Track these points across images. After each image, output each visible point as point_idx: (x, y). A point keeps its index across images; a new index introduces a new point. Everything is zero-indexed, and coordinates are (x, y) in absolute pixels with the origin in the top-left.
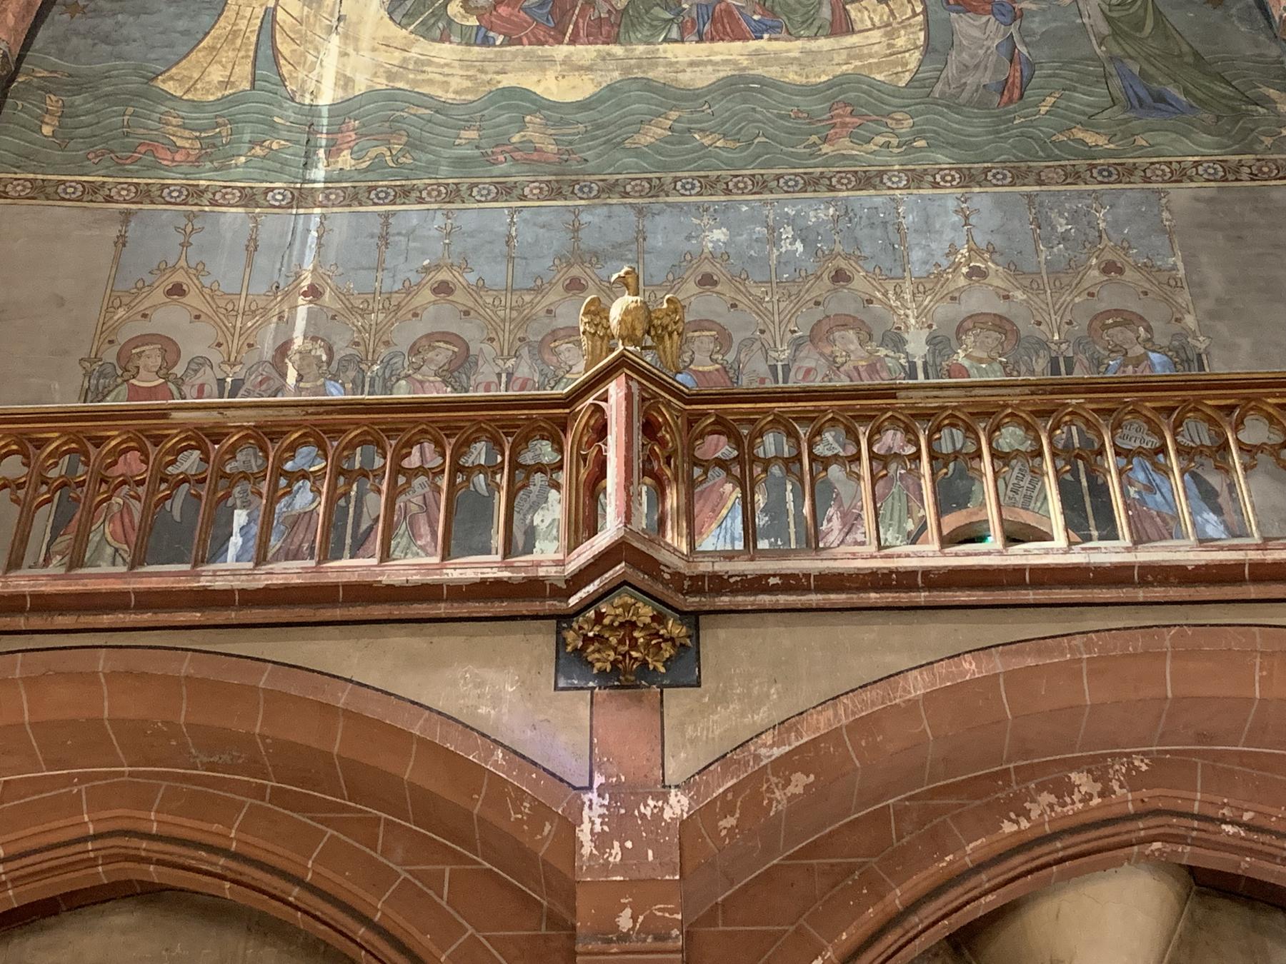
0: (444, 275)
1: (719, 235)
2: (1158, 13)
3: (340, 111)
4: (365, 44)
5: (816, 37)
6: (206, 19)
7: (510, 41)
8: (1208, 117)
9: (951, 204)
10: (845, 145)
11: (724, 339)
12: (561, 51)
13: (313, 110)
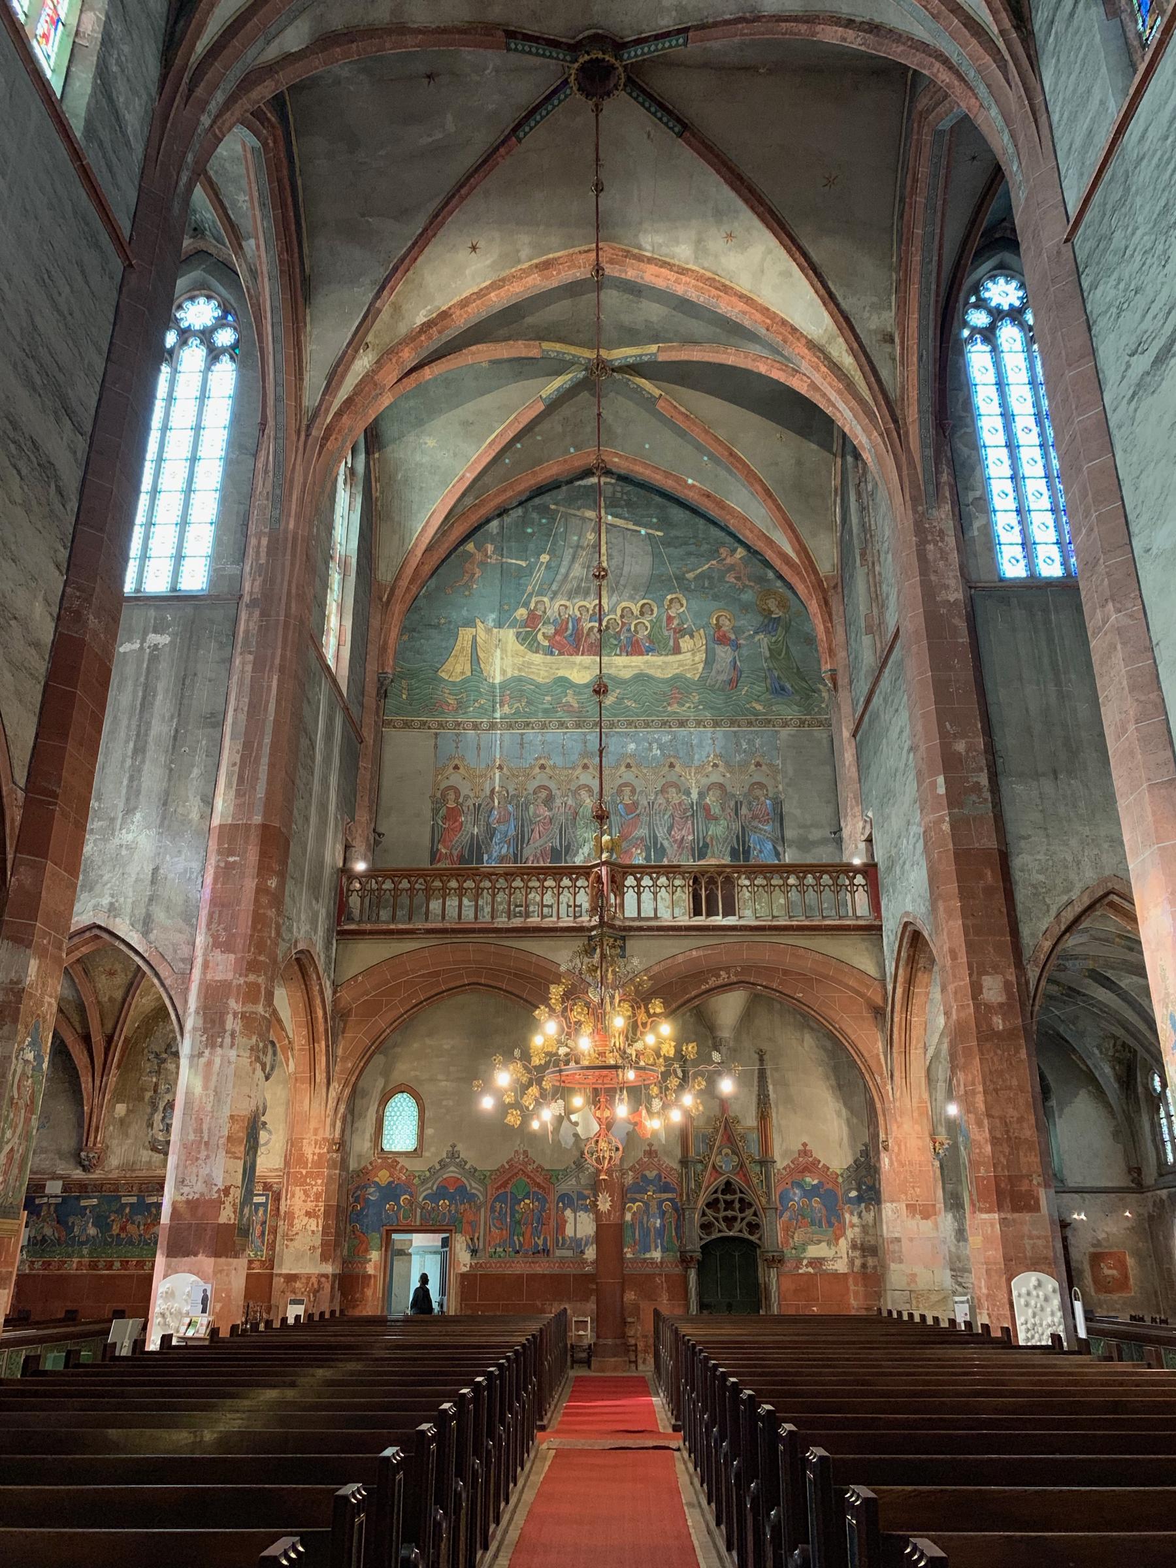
0: (542, 761)
1: (633, 746)
2: (787, 647)
3: (504, 685)
4: (509, 654)
5: (667, 655)
6: (452, 641)
7: (561, 654)
8: (798, 698)
9: (709, 735)
10: (675, 708)
11: (633, 791)
12: (578, 659)
13: (493, 686)
